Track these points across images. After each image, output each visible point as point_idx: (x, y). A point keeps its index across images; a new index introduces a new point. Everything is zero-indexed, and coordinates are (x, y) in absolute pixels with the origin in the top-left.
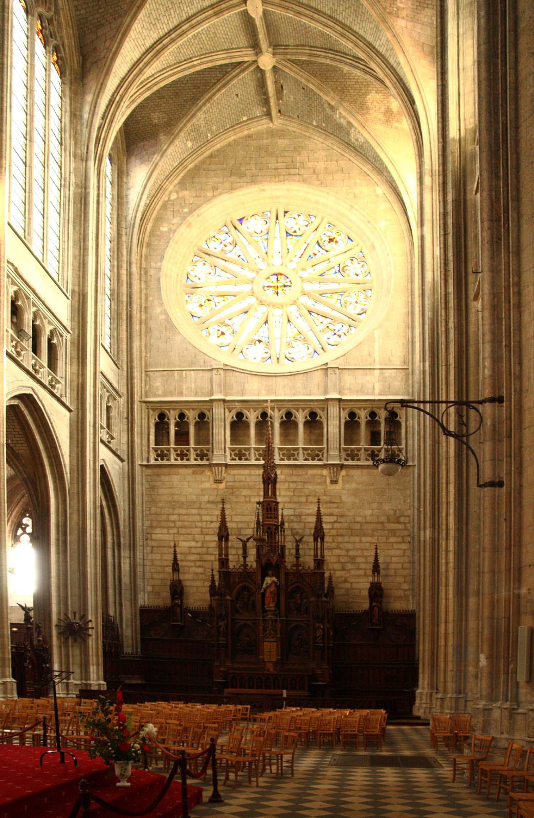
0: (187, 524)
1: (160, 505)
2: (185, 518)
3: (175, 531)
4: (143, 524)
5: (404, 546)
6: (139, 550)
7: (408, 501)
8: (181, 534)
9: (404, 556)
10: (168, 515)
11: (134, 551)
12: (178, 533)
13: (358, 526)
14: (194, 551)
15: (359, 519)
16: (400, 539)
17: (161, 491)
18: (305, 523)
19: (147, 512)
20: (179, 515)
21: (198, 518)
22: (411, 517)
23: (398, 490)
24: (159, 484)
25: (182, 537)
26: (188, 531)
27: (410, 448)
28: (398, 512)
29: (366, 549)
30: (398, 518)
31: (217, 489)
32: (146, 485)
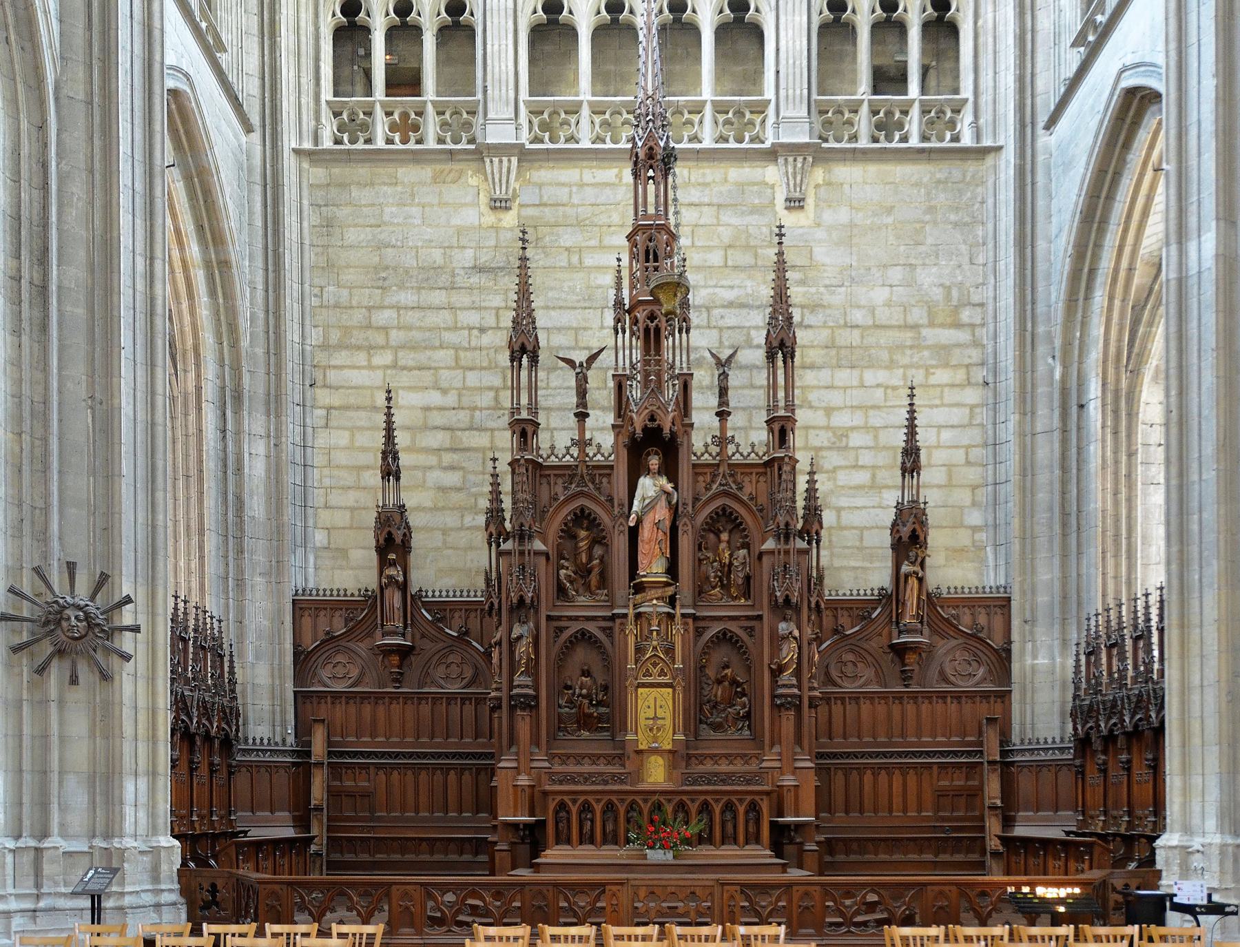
0: (417, 335)
1: (349, 276)
2: (411, 317)
3: (385, 358)
4: (303, 337)
5: (972, 396)
6: (292, 414)
7: (981, 260)
8: (404, 368)
9: (970, 425)
10: (369, 309)
11: (278, 416)
12: (394, 366)
13: (854, 337)
14: (437, 419)
15: (858, 316)
16: (960, 375)
17: (352, 236)
18: (721, 329)
19: (315, 302)
20: (398, 308)
21: (444, 318)
22: (990, 308)
23: (956, 225)
24: (343, 213)
25: (405, 379)
26: (422, 357)
27: (986, 99)
28: (955, 293)
29: (874, 407)
30: (956, 309)
31: (496, 229)
32: (311, 218)
